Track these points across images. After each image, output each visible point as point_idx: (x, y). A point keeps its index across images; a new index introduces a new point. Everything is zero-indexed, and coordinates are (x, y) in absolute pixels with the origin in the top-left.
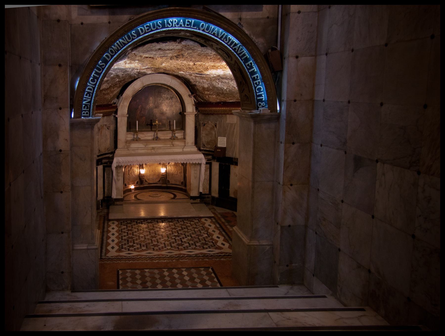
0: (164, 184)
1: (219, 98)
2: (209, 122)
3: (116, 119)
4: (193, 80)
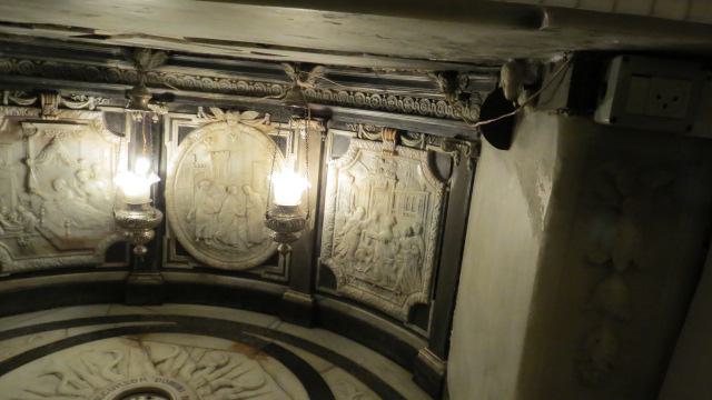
0: (298, 289)
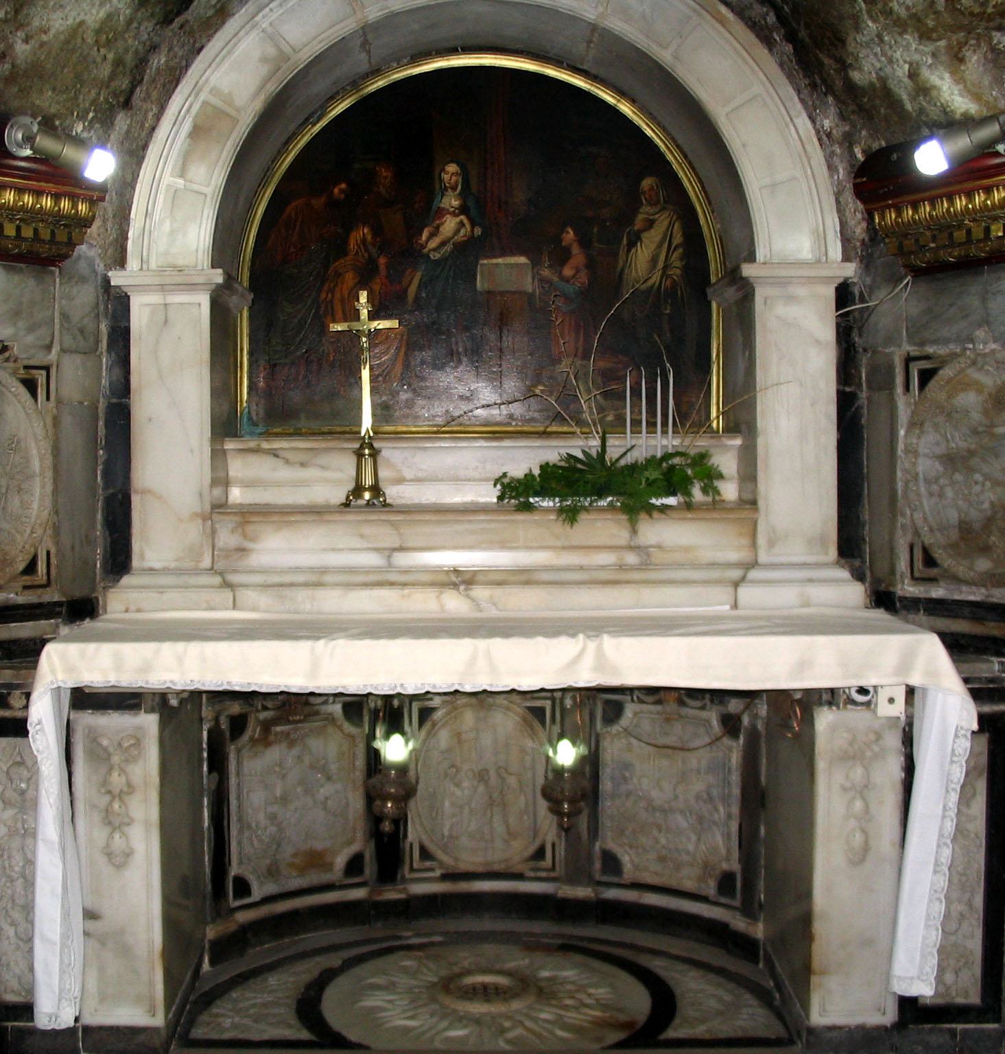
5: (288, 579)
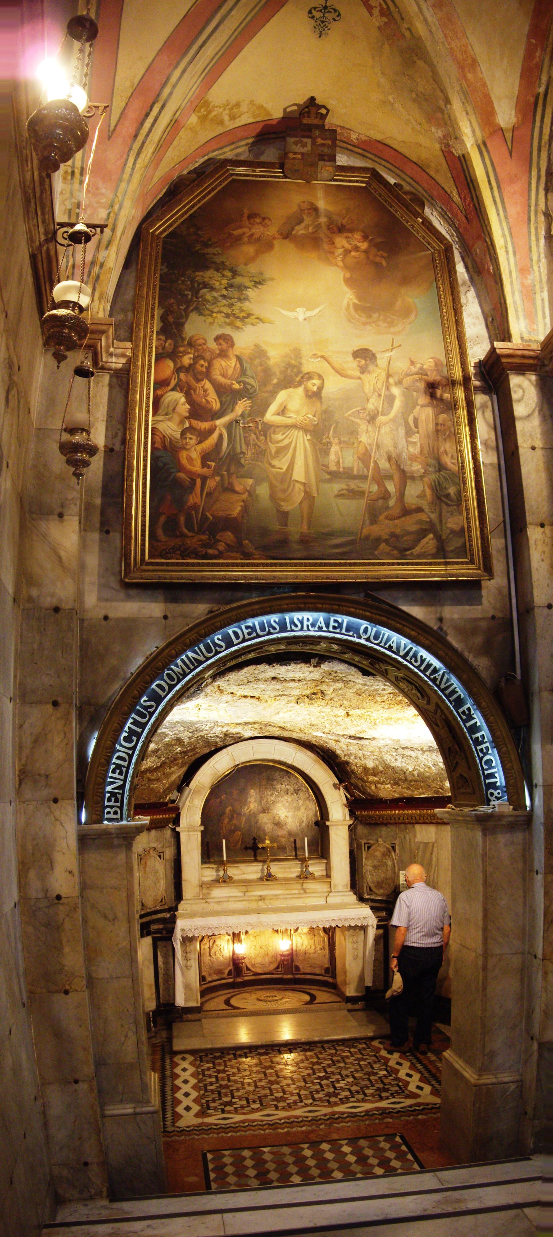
0: (288, 974)
1: (399, 789)
2: (380, 840)
3: (177, 836)
4: (343, 751)
5: (221, 900)
